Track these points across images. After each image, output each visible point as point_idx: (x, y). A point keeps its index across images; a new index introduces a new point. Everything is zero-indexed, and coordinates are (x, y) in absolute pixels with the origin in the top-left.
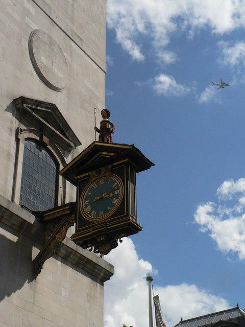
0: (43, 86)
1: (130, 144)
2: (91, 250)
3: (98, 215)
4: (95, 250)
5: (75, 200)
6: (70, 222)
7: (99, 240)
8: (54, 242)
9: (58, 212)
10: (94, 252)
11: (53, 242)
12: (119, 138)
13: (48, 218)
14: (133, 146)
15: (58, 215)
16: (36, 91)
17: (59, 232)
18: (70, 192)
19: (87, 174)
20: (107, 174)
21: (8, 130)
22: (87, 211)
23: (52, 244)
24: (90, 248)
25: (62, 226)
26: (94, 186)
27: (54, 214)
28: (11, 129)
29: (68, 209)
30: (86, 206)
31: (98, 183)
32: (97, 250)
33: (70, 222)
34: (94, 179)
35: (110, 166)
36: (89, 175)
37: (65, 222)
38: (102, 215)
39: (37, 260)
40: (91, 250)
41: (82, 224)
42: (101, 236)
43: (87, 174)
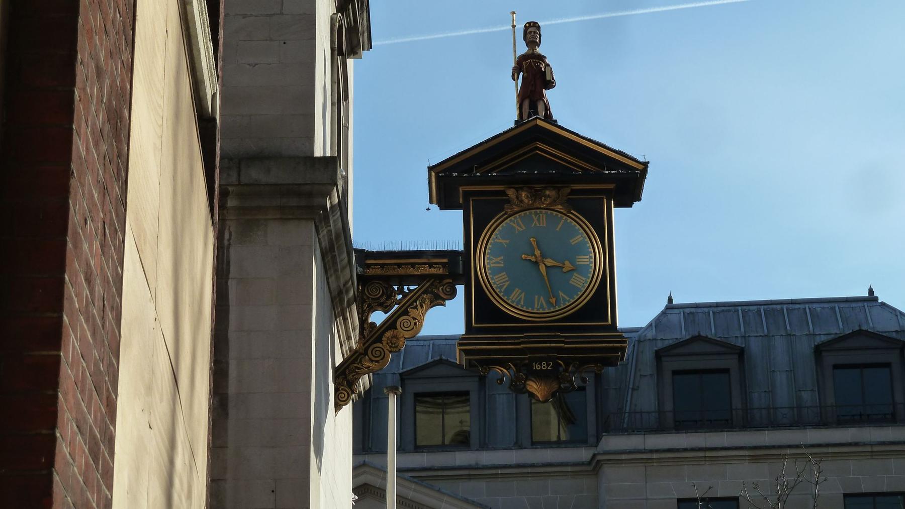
1: (642, 160)
5: (459, 245)
7: (537, 367)
9: (413, 265)
11: (389, 334)
13: (378, 271)
17: (406, 313)
20: (559, 207)
25: (415, 301)
27: (399, 265)
29: (444, 265)
34: (516, 209)
36: (503, 193)
38: (542, 307)
39: (345, 370)
41: (482, 310)
42: (547, 359)
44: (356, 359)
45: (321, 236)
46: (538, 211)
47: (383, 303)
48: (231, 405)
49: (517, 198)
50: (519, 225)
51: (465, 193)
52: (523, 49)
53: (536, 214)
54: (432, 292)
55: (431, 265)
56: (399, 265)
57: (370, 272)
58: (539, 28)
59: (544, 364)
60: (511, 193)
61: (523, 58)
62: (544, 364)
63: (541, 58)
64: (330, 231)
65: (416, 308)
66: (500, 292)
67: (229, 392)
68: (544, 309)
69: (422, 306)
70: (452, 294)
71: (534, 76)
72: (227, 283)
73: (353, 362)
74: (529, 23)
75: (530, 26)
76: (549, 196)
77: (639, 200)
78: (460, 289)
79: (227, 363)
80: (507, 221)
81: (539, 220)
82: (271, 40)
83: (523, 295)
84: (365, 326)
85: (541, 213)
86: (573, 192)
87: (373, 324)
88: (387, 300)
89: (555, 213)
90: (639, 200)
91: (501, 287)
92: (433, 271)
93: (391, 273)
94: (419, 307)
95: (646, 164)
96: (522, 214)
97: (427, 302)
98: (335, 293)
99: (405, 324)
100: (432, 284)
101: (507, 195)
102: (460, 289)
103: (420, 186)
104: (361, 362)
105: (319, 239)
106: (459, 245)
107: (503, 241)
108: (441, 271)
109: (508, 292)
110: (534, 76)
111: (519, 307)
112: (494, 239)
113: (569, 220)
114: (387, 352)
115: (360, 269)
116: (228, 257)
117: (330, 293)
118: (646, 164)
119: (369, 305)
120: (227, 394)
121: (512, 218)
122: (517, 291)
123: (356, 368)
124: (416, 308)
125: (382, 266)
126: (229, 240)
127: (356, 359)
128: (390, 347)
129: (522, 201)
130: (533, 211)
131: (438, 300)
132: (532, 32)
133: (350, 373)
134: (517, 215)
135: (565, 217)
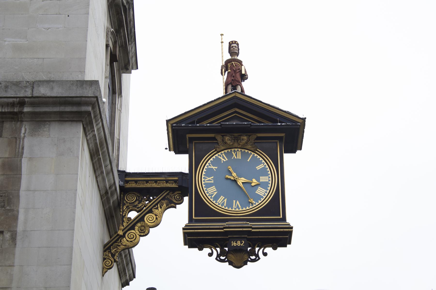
1: (301, 116)
2: (210, 255)
3: (230, 204)
4: (218, 256)
5: (186, 170)
6: (171, 202)
7: (234, 244)
8: (142, 226)
9: (156, 181)
10: (216, 259)
11: (139, 225)
13: (134, 185)
15: (154, 185)
17: (151, 211)
23: (136, 228)
25: (157, 204)
26: (222, 157)
27: (147, 181)
29: (175, 181)
30: (208, 185)
31: (229, 155)
32: (222, 258)
33: (171, 202)
35: (254, 136)
36: (214, 139)
37: (163, 199)
38: (238, 207)
40: (210, 255)
41: (200, 209)
42: (240, 239)
44: (118, 240)
45: (88, 138)
46: (236, 150)
47: (137, 205)
48: (19, 238)
49: (223, 140)
50: (223, 158)
51: (189, 138)
52: (228, 57)
53: (234, 151)
54: (168, 199)
55: (167, 181)
56: (147, 181)
57: (128, 186)
58: (238, 44)
59: (239, 242)
60: (219, 138)
61: (228, 62)
62: (239, 242)
63: (240, 62)
64: (95, 135)
65: (157, 208)
66: (211, 198)
67: (18, 231)
68: (239, 209)
69: (161, 208)
70: (181, 202)
71: (234, 72)
72: (21, 160)
73: (116, 242)
74: (232, 42)
75: (233, 43)
76: (243, 139)
77: (301, 149)
78: (186, 199)
79: (18, 212)
80: (217, 155)
81: (236, 155)
82: (60, 14)
83: (226, 200)
84: (124, 219)
85: (238, 150)
86: (258, 138)
87: (130, 218)
88: (139, 203)
89: (246, 151)
90: (301, 149)
91: (212, 195)
92: (169, 185)
93: (142, 186)
94: (159, 209)
95: (304, 120)
96: (226, 151)
97: (165, 205)
98: (103, 192)
99: (150, 219)
100: (168, 194)
101: (216, 140)
102: (186, 199)
103: (162, 137)
104: (121, 241)
105: (87, 140)
106: (186, 170)
107: (214, 168)
108: (174, 185)
109: (216, 198)
110: (234, 72)
111: (223, 207)
112: (207, 166)
113: (256, 155)
114: (138, 236)
115: (122, 183)
116: (23, 144)
117: (100, 191)
118: (304, 120)
119: (127, 207)
120: (16, 231)
121: (220, 153)
122: (222, 198)
123: (117, 245)
124: (157, 208)
125: (136, 182)
126: (24, 134)
127: (118, 240)
128: (140, 233)
129: (226, 143)
130: (233, 150)
131: (172, 204)
132: (233, 48)
133: (113, 249)
134: (223, 152)
135: (253, 153)
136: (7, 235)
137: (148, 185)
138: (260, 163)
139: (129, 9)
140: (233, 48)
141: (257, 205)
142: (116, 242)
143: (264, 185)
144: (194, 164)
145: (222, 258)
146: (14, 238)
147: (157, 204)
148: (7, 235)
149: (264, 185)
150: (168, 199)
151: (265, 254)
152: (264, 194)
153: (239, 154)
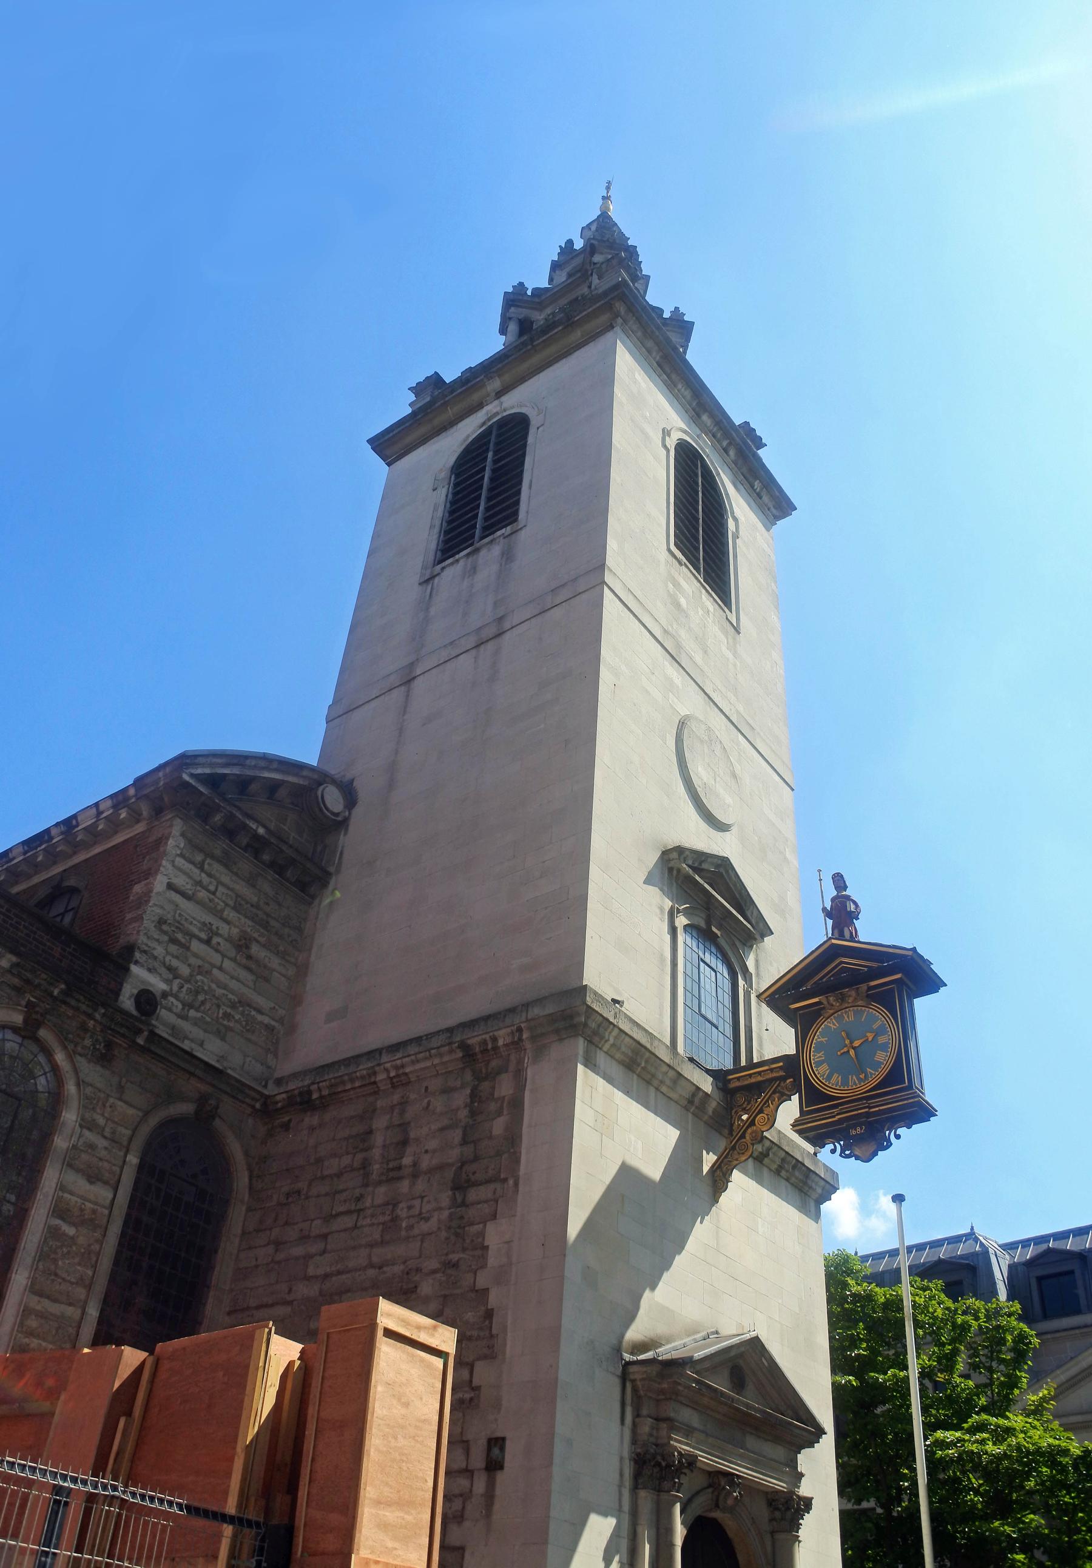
0: (703, 825)
2: (833, 1151)
3: (845, 1082)
4: (843, 1151)
5: (792, 1051)
7: (854, 1132)
9: (759, 1073)
11: (749, 1131)
12: (870, 931)
13: (737, 1084)
14: (914, 949)
15: (759, 1079)
16: (697, 836)
17: (761, 1111)
18: (774, 1038)
19: (816, 1000)
20: (860, 1003)
21: (658, 911)
22: (820, 1072)
23: (748, 1136)
24: (831, 1146)
25: (767, 1101)
27: (750, 1075)
28: (661, 909)
30: (819, 1064)
32: (847, 1152)
33: (782, 1094)
35: (864, 987)
37: (774, 1092)
40: (833, 1151)
43: (816, 1000)
54: (779, 1092)
59: (858, 1129)
62: (858, 1129)
71: (842, 913)
92: (775, 1075)
93: (746, 1082)
106: (792, 1051)
108: (782, 1073)
109: (829, 1078)
110: (842, 913)
122: (835, 1075)
132: (839, 881)
136: (511, 1182)
137: (753, 1080)
138: (877, 1019)
139: (727, 872)
140: (839, 881)
141: (876, 1076)
142: (726, 1157)
143: (884, 1047)
144: (801, 1040)
145: (847, 1152)
146: (516, 1184)
147: (767, 1101)
148: (511, 1182)
149: (884, 1047)
150: (779, 1092)
151: (898, 1137)
152: (884, 1059)
153: (851, 1014)
